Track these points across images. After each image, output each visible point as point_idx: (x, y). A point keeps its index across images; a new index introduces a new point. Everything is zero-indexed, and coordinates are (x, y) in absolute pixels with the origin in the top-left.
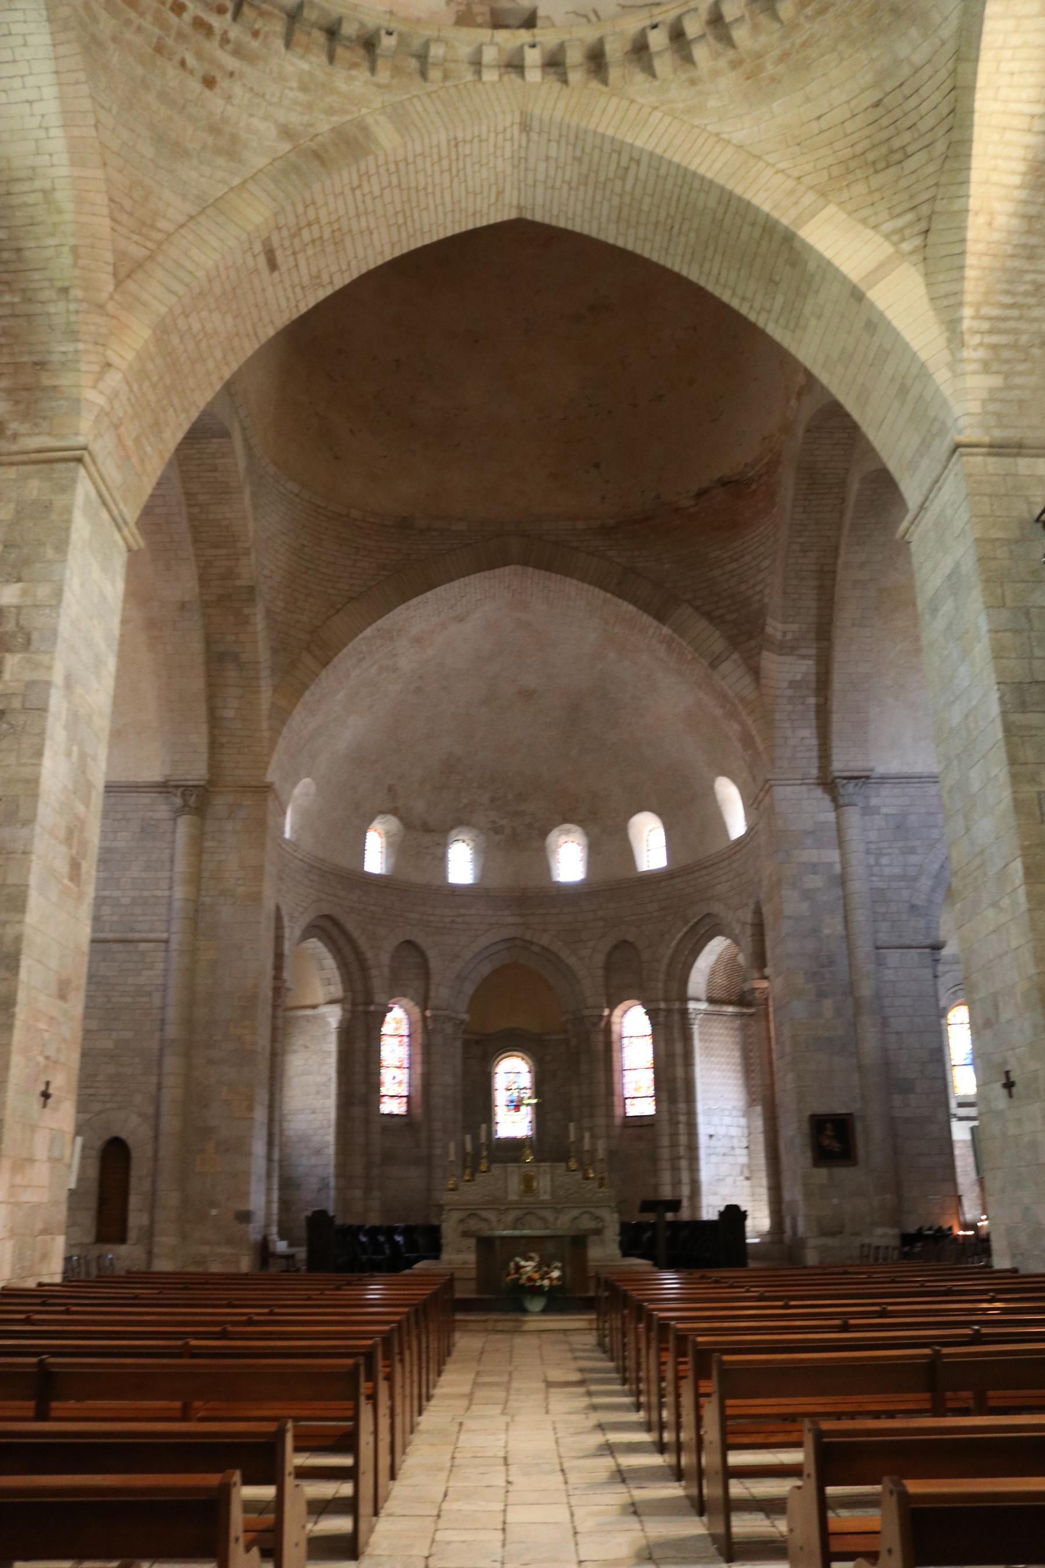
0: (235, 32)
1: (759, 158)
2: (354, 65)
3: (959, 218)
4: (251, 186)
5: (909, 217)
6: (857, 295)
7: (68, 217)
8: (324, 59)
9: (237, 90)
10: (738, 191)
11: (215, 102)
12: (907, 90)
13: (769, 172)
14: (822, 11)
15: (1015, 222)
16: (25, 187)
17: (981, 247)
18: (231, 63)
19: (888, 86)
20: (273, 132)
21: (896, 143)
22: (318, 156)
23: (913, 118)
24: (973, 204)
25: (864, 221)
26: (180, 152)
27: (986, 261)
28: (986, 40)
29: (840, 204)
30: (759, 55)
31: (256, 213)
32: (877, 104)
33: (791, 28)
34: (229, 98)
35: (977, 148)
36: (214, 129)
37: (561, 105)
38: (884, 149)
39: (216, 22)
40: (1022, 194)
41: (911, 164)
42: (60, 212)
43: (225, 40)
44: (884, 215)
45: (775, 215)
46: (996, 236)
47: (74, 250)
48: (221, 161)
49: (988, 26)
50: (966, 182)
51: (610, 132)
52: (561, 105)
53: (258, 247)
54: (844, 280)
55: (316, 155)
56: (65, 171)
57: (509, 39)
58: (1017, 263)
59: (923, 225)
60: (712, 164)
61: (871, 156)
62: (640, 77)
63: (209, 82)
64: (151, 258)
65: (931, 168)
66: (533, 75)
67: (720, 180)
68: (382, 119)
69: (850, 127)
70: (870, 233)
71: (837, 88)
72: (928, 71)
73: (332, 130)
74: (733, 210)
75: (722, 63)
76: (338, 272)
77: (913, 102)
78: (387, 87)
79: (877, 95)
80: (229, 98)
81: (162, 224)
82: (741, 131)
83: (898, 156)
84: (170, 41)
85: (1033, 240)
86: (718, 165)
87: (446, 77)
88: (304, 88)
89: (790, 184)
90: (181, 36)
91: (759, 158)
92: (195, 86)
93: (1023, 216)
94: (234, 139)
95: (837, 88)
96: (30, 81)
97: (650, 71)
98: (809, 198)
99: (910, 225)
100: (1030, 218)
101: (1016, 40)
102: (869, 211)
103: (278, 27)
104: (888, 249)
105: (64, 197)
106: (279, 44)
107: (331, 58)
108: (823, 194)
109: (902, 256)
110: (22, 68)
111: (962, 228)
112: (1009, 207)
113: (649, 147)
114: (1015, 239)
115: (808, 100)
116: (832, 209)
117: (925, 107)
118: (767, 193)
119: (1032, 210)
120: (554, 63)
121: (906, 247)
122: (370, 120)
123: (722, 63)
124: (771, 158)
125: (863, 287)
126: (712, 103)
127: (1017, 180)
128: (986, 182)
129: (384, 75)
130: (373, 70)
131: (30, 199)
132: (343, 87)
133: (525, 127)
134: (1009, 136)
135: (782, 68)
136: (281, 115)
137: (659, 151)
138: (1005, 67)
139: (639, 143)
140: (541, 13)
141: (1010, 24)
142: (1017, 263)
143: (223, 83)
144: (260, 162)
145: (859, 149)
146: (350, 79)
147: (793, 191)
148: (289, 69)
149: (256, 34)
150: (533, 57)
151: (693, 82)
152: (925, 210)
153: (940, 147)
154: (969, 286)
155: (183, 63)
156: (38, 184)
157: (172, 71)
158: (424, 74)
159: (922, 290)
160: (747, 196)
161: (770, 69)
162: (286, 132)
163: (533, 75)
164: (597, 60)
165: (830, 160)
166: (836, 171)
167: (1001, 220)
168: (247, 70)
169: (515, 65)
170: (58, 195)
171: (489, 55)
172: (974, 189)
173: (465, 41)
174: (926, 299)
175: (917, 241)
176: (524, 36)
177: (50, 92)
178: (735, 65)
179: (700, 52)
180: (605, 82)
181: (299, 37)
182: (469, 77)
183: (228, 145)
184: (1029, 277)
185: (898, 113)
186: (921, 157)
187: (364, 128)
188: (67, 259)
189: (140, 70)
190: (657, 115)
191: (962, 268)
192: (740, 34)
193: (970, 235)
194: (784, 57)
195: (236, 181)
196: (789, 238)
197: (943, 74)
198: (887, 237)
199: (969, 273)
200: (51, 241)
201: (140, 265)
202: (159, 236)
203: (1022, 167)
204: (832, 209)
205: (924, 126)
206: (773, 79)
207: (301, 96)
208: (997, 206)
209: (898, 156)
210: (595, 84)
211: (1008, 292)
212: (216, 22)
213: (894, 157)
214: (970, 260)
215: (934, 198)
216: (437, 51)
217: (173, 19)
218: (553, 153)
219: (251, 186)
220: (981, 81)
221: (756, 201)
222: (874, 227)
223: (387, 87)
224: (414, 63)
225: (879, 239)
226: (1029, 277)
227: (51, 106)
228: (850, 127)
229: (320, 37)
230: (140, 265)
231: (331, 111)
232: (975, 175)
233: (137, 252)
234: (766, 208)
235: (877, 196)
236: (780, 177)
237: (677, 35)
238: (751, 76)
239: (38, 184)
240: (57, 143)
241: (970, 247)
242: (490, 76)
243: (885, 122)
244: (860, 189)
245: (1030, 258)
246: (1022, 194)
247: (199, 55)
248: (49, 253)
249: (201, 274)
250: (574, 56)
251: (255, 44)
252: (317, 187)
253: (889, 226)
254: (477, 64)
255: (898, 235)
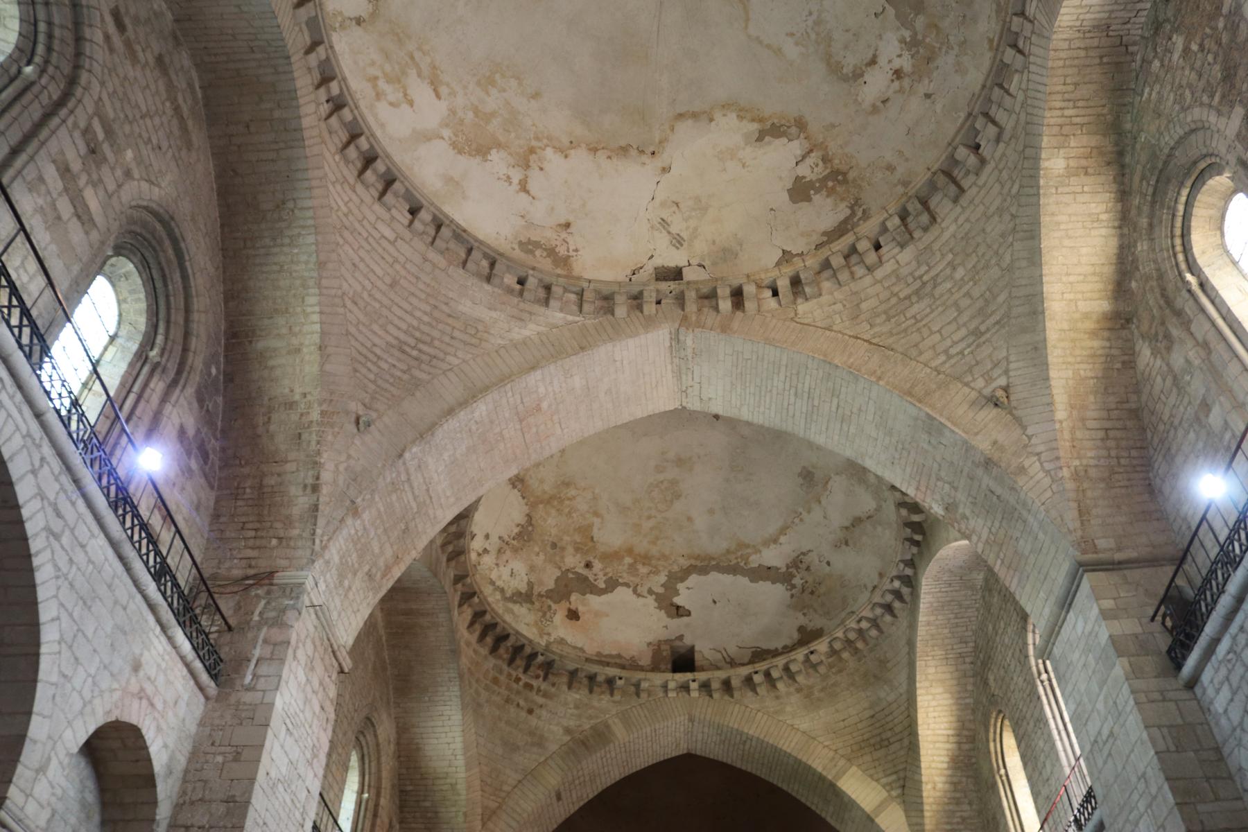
0: (544, 686)
1: (814, 739)
2: (603, 693)
3: (918, 784)
4: (550, 762)
5: (894, 777)
6: (870, 819)
7: (463, 797)
8: (587, 691)
9: (544, 713)
10: (804, 760)
11: (533, 721)
12: (886, 712)
13: (820, 747)
14: (840, 671)
15: (947, 786)
16: (442, 782)
17: (931, 800)
18: (540, 700)
19: (877, 709)
20: (561, 731)
21: (884, 737)
22: (584, 743)
23: (891, 725)
24: (924, 779)
25: (871, 776)
26: (514, 748)
27: (934, 807)
28: (919, 704)
29: (859, 766)
30: (810, 687)
31: (553, 779)
32: (873, 716)
33: (825, 677)
34: (539, 718)
35: (922, 752)
36: (532, 734)
37: (710, 710)
38: (878, 739)
39: (535, 683)
40: (949, 772)
41: (893, 748)
42: (459, 795)
43: (539, 690)
44: (881, 775)
45: (824, 773)
46: (938, 794)
47: (465, 814)
48: (535, 749)
49: (919, 699)
50: (919, 767)
51: (736, 726)
52: (710, 710)
53: (553, 794)
54: (863, 810)
55: (584, 743)
56: (463, 775)
57: (681, 677)
58: (951, 807)
59: (901, 782)
60: (790, 744)
61: (872, 741)
62: (750, 694)
63: (530, 712)
64: (499, 807)
65: (902, 753)
66: (695, 694)
67: (794, 754)
68: (616, 720)
69: (860, 726)
70: (874, 783)
71: (852, 707)
72: (895, 705)
73: (591, 728)
74: (801, 770)
75: (792, 689)
76: (590, 792)
77: (890, 718)
78: (619, 702)
79: (872, 713)
80: (539, 718)
81: (506, 788)
82: (804, 724)
83: (886, 743)
84: (513, 696)
85: (958, 795)
86: (793, 744)
87: (649, 695)
88: (577, 707)
89: (831, 754)
90: (518, 693)
91: (814, 739)
92: (523, 714)
93: (951, 783)
94: (542, 737)
95: (852, 707)
96: (450, 735)
97: (754, 690)
98: (842, 762)
99: (894, 781)
100: (954, 784)
101: (934, 703)
102: (872, 771)
103: (565, 679)
104: (885, 794)
105: (461, 787)
106: (565, 688)
107: (591, 691)
108: (849, 760)
109: (893, 798)
110: (447, 729)
111: (920, 790)
112: (943, 779)
113: (756, 735)
114: (949, 795)
115: (837, 711)
116: (854, 768)
117: (896, 721)
118: (819, 760)
119: (955, 779)
120: (705, 686)
121: (894, 793)
122: (610, 722)
123: (792, 689)
124: (821, 739)
125: (873, 816)
126: (788, 709)
127: (945, 766)
128: (930, 767)
129: (617, 697)
130: (612, 694)
131: (444, 788)
132: (595, 703)
133: (691, 720)
134: (937, 745)
135: (822, 695)
136: (565, 723)
137: (762, 737)
138: (931, 715)
139: (751, 732)
140: (697, 648)
141: (930, 697)
142: (951, 807)
143: (537, 711)
144: (554, 747)
145: (866, 737)
146: (600, 700)
147: (833, 758)
148: (570, 699)
149: (553, 685)
150: (694, 686)
151: (777, 698)
152: (902, 774)
153: (906, 742)
154: (927, 821)
155: (518, 705)
156: (448, 781)
157: (512, 710)
158: (638, 695)
159: (904, 819)
160: (809, 762)
161: (817, 694)
162: (568, 731)
163: (695, 694)
164: (727, 685)
165: (852, 742)
166: (855, 747)
167: (940, 786)
168: (549, 702)
169: (685, 688)
170: (459, 787)
171: (672, 685)
172: (923, 771)
173: (658, 679)
174: (906, 825)
175: (899, 791)
176: (689, 676)
177: (459, 739)
178: (799, 690)
179: (780, 685)
180: (732, 696)
181: (575, 684)
182: (661, 694)
183: (538, 741)
184: (958, 814)
185: (883, 722)
186: (897, 745)
187: (608, 727)
188: (461, 819)
189: (498, 713)
190: (760, 714)
191: (922, 811)
192: (800, 678)
193: (925, 794)
194: (822, 690)
195: (542, 759)
196: (832, 787)
197: (903, 708)
198: (884, 786)
199: (927, 814)
200: (454, 809)
201: (494, 812)
202: (503, 794)
203: (946, 759)
204: (854, 768)
205: (897, 730)
206: (819, 700)
207: (576, 712)
208: (937, 779)
209: (886, 743)
210: (727, 697)
211: (948, 823)
212: (535, 683)
213: (883, 744)
214: (926, 807)
215: (905, 769)
216: (644, 685)
217: (515, 686)
218: (706, 730)
219: (550, 762)
220: (920, 721)
221: (814, 766)
222: (877, 781)
223: (619, 702)
224: (633, 689)
225: (879, 787)
226: (958, 814)
227: (458, 745)
228: (860, 726)
229: (585, 681)
230: (494, 812)
231: (590, 718)
232: (923, 765)
233: (494, 805)
234: (820, 769)
235: (877, 763)
236: (826, 751)
237: (767, 674)
238: (808, 696)
239: (448, 781)
240: (460, 761)
241: (925, 800)
242: (671, 694)
243: (877, 725)
244: (868, 758)
245: (957, 804)
246: (949, 772)
247: (526, 700)
248: (453, 814)
249: (525, 815)
250: (715, 685)
251: (553, 690)
252: (584, 762)
253: (884, 780)
254: (665, 687)
255: (888, 787)
